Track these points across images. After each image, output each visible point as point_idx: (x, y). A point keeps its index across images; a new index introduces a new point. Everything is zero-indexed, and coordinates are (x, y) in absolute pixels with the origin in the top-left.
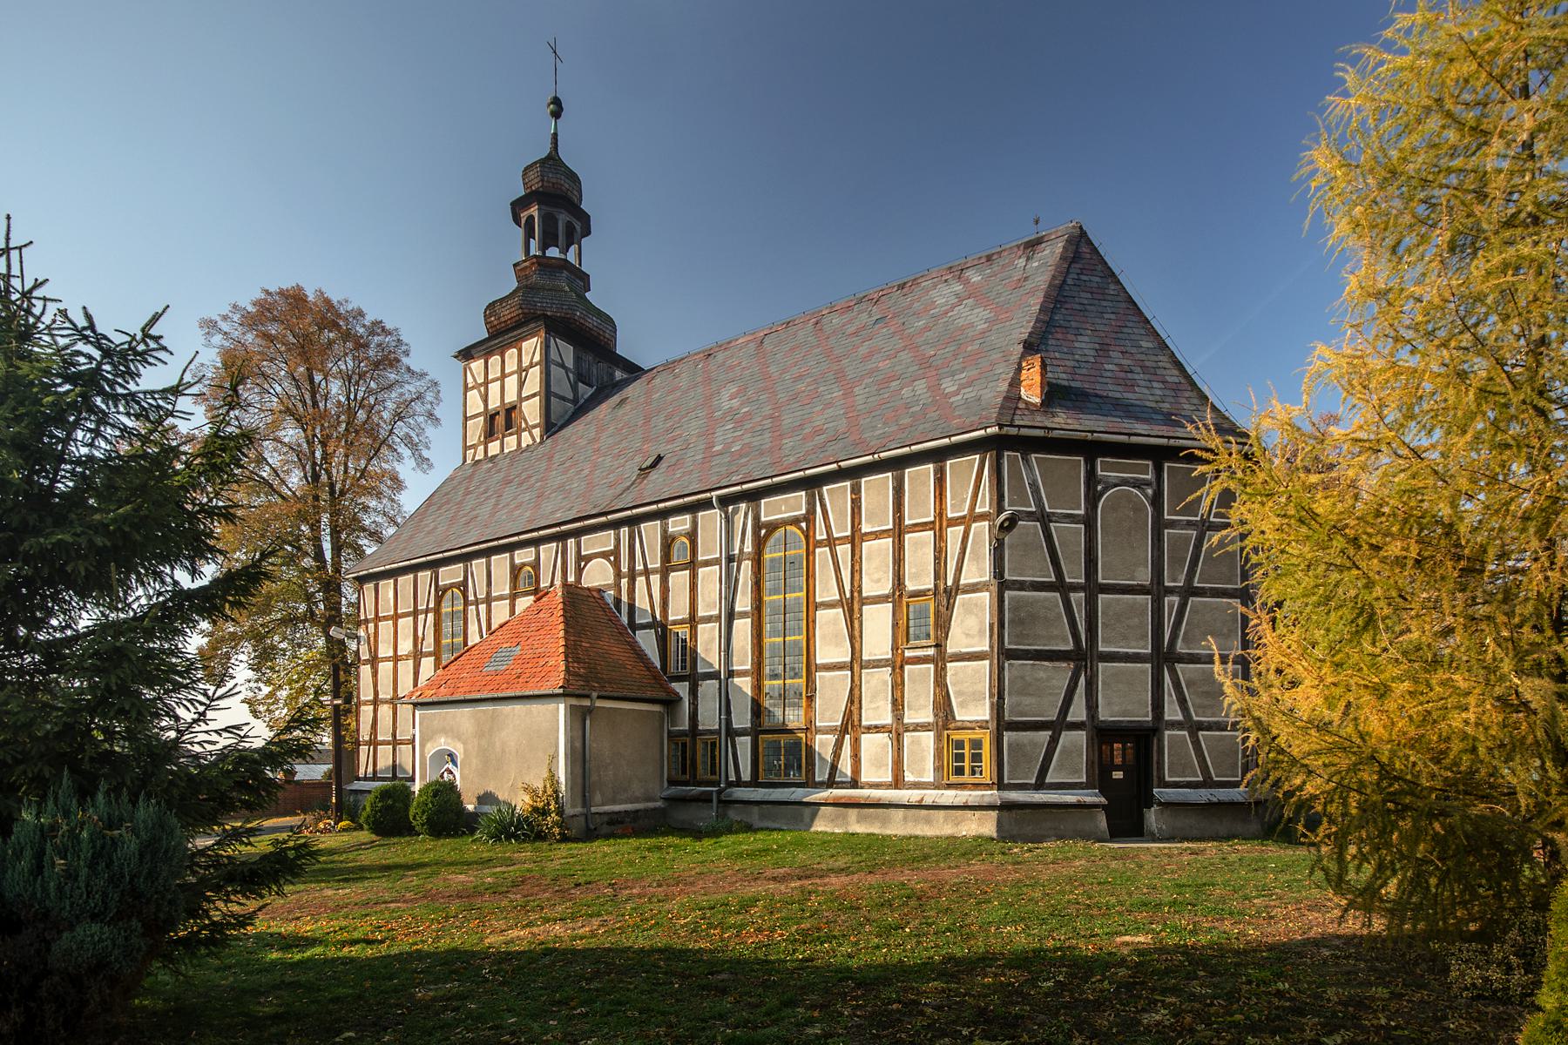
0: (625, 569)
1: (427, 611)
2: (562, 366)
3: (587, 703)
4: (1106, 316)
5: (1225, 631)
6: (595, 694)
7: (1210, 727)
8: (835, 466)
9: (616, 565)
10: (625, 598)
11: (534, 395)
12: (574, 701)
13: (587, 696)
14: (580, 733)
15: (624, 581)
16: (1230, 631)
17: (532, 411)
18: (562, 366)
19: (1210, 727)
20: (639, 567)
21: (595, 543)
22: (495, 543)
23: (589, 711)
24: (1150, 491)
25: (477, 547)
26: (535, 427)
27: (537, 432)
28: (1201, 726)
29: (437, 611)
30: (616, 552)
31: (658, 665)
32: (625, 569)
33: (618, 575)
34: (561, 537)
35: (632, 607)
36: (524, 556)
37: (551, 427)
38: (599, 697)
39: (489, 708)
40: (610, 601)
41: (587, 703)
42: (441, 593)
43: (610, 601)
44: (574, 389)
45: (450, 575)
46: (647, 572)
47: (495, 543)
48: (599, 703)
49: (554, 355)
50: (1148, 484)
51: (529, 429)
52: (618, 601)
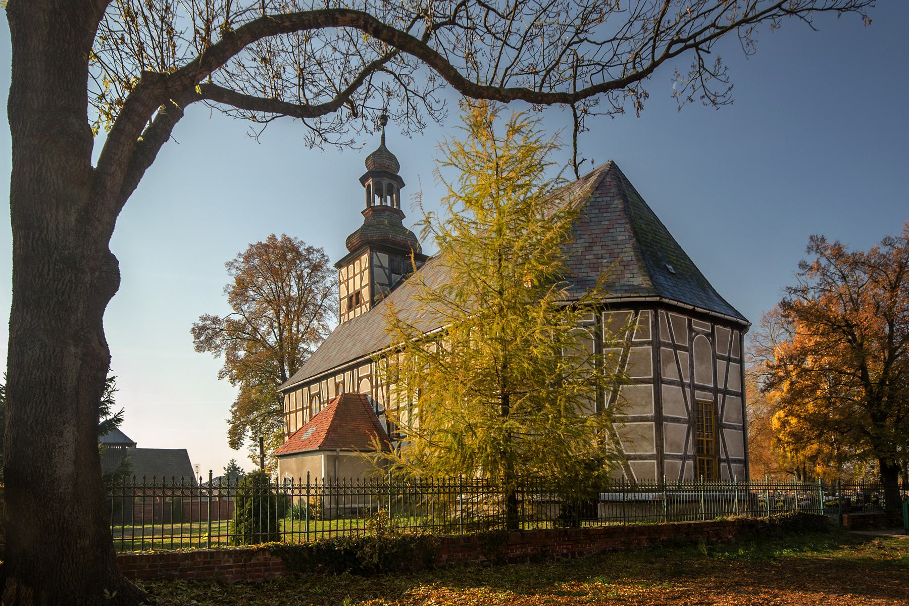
0: (374, 384)
1: (307, 408)
2: (381, 267)
3: (335, 454)
4: (602, 223)
5: (644, 403)
6: (338, 449)
7: (635, 458)
8: (440, 329)
9: (371, 381)
10: (374, 399)
11: (366, 285)
12: (329, 453)
13: (335, 450)
14: (333, 469)
15: (374, 390)
16: (646, 402)
17: (366, 294)
18: (381, 267)
19: (635, 458)
20: (379, 383)
21: (365, 370)
22: (333, 370)
23: (336, 458)
24: (593, 329)
25: (323, 374)
26: (367, 302)
27: (368, 305)
28: (629, 458)
29: (310, 407)
30: (371, 375)
31: (387, 433)
32: (374, 384)
33: (372, 387)
34: (351, 368)
35: (377, 402)
36: (339, 378)
37: (373, 303)
38: (341, 451)
39: (300, 457)
40: (369, 400)
41: (335, 454)
42: (312, 397)
43: (369, 400)
44: (389, 278)
45: (314, 389)
46: (382, 385)
47: (333, 370)
48: (341, 454)
49: (376, 262)
50: (592, 324)
51: (365, 303)
52: (372, 400)
